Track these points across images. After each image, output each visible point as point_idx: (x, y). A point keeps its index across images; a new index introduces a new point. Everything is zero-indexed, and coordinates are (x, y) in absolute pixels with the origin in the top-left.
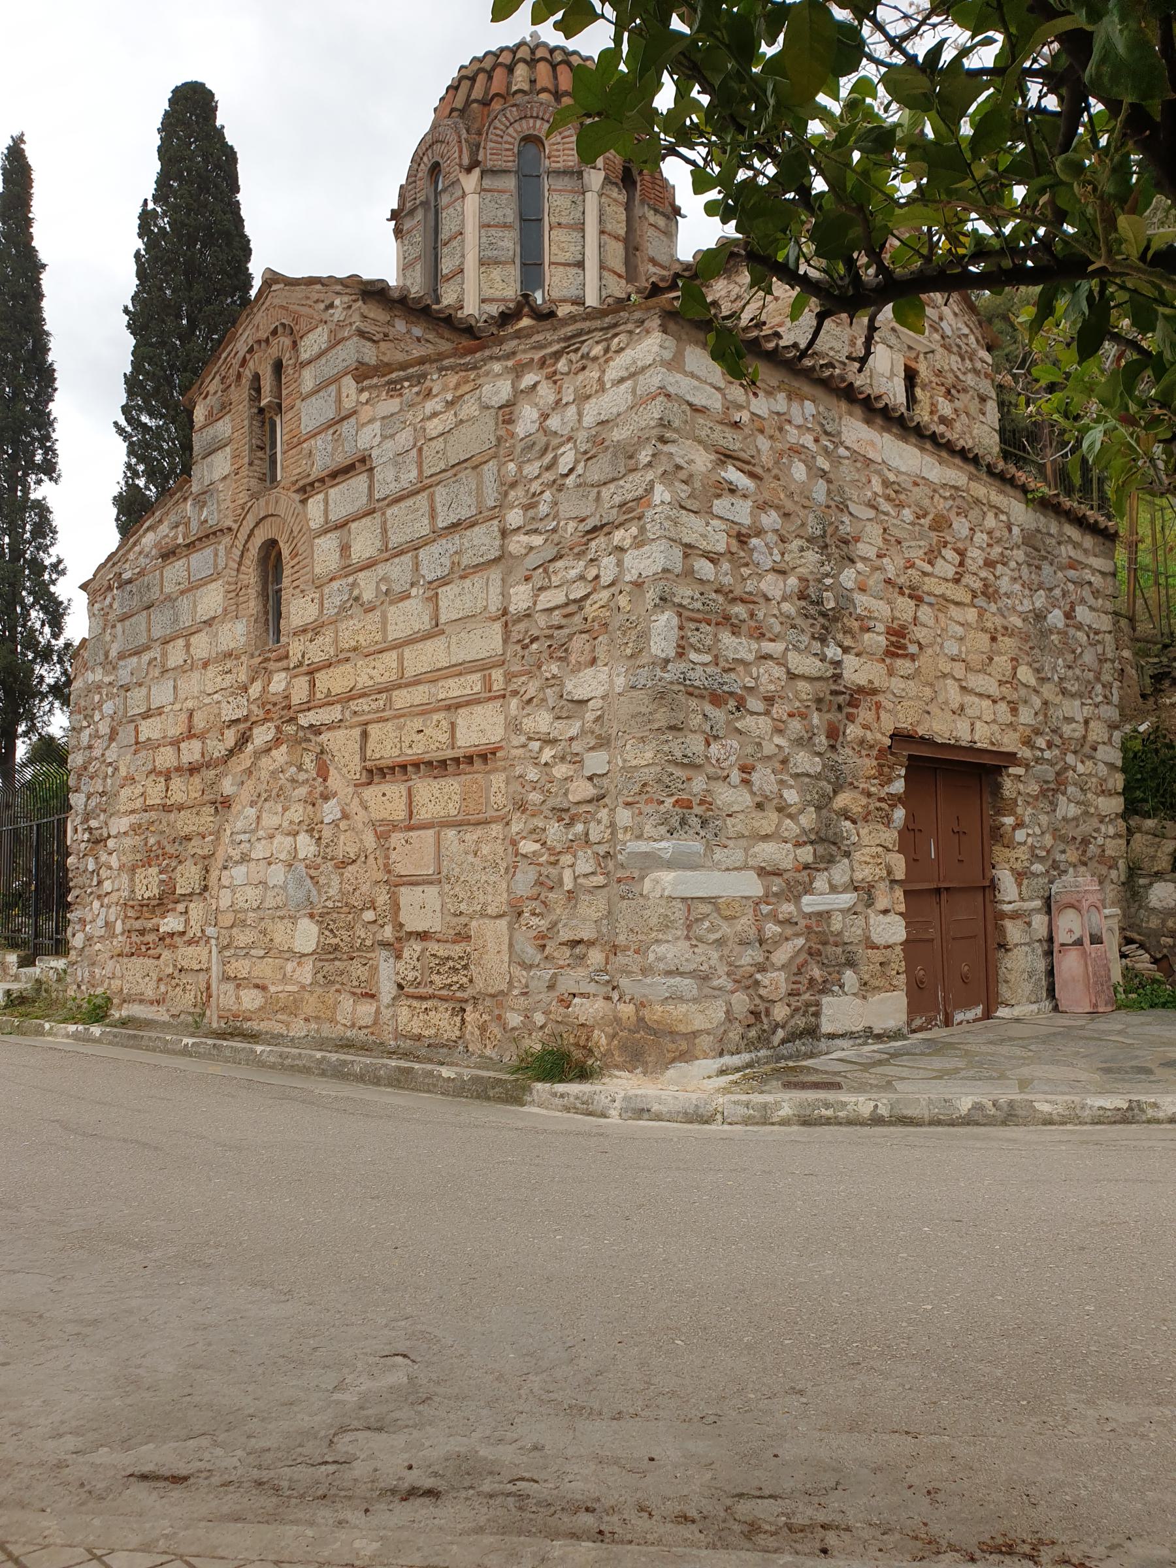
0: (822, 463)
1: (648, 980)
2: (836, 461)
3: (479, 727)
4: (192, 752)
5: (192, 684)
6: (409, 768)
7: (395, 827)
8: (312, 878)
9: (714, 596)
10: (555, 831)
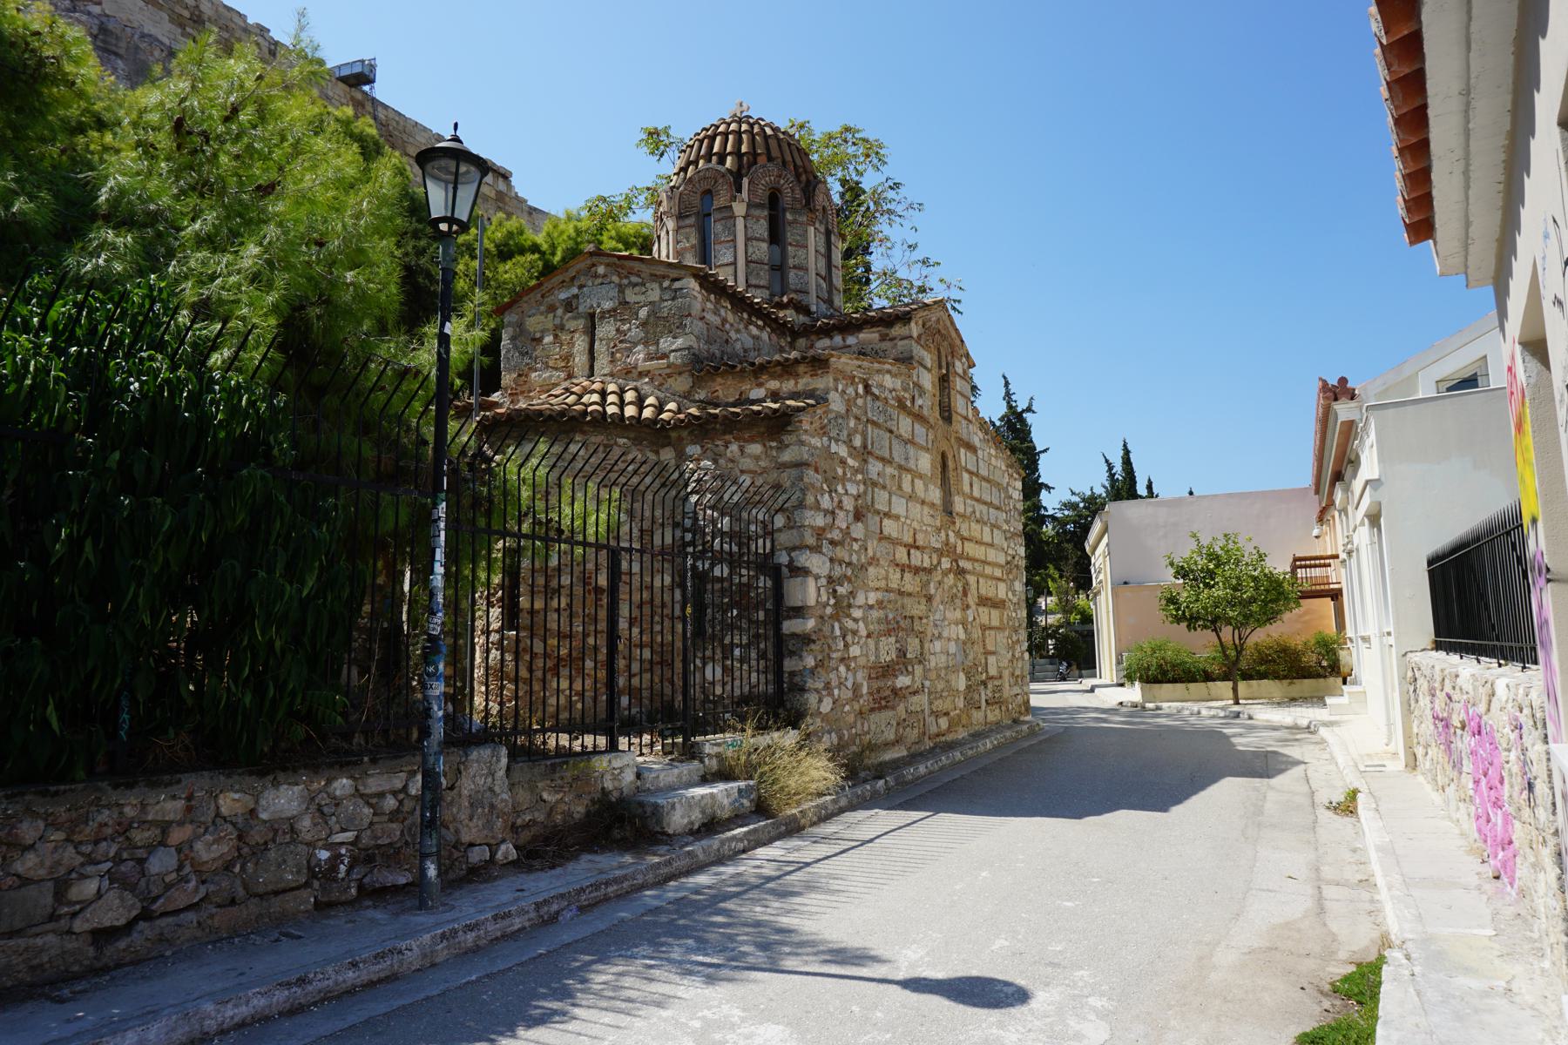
4: (917, 558)
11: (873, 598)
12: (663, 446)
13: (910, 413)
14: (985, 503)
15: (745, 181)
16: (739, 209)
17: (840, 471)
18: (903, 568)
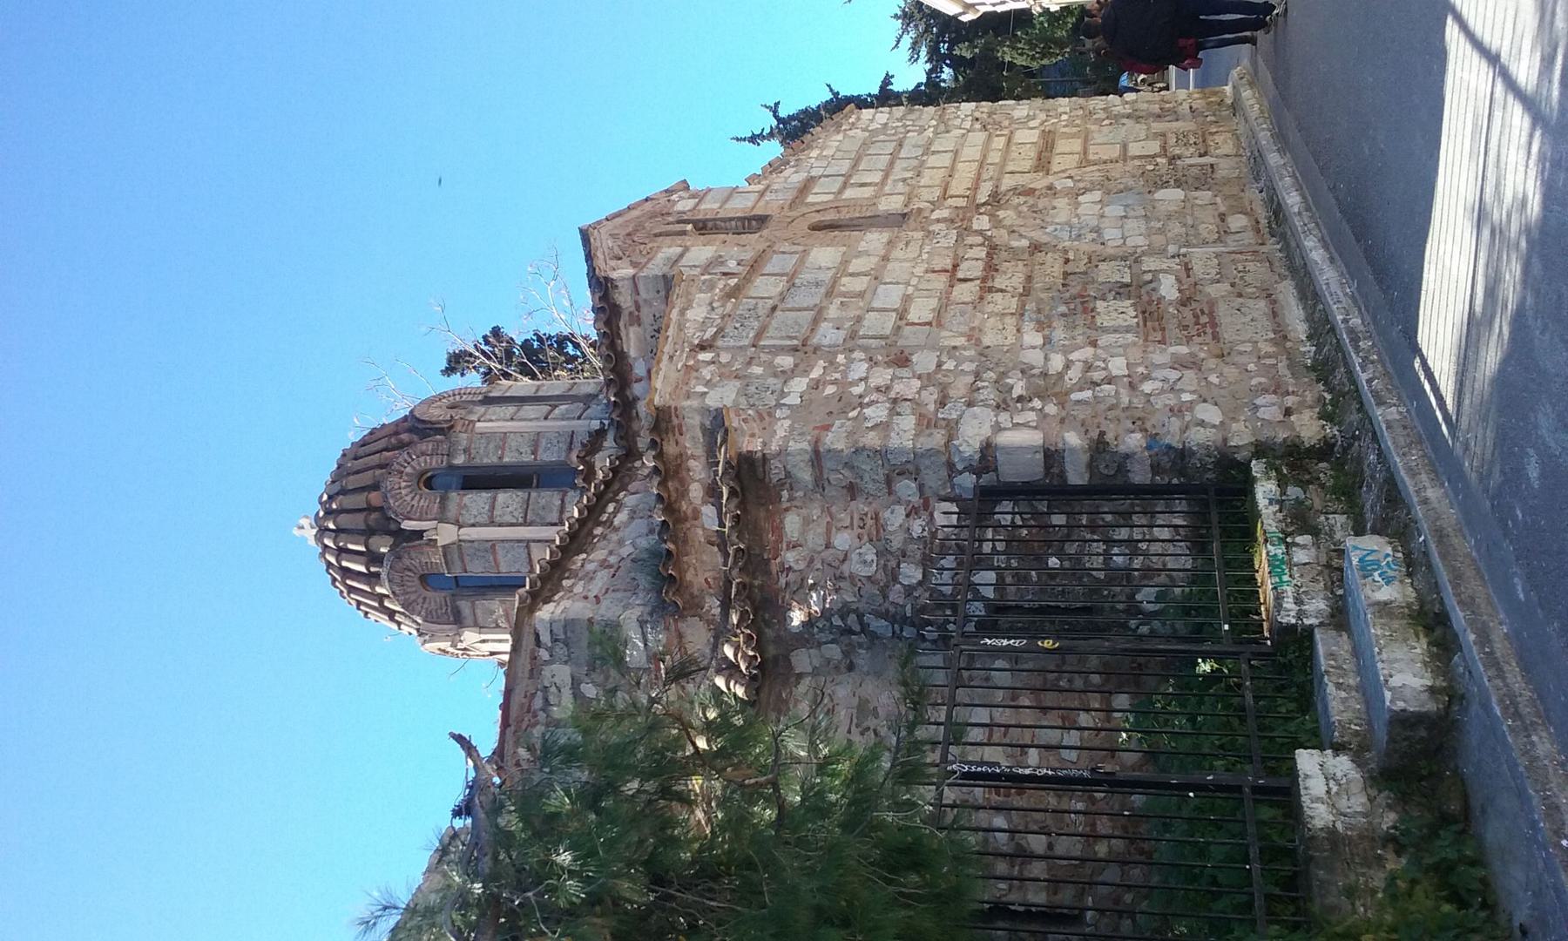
11: (1033, 338)
12: (790, 667)
13: (747, 280)
14: (892, 164)
15: (407, 525)
16: (446, 534)
17: (830, 389)
18: (987, 289)
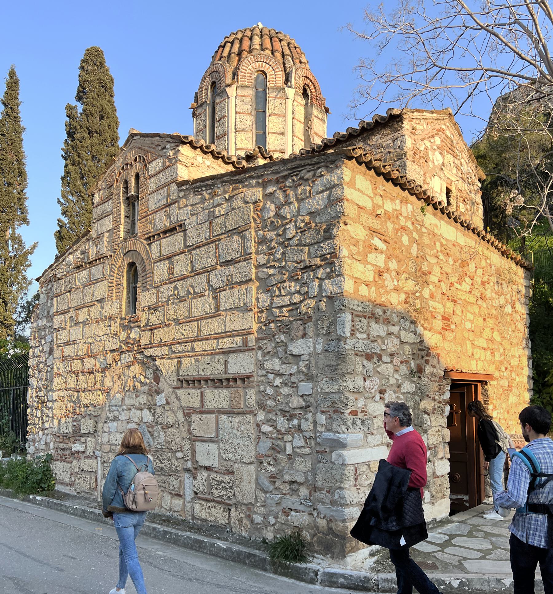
0: (415, 235)
1: (335, 508)
2: (421, 234)
3: (240, 365)
4: (89, 363)
5: (91, 330)
6: (202, 382)
7: (194, 411)
8: (150, 432)
9: (368, 303)
10: (282, 422)
